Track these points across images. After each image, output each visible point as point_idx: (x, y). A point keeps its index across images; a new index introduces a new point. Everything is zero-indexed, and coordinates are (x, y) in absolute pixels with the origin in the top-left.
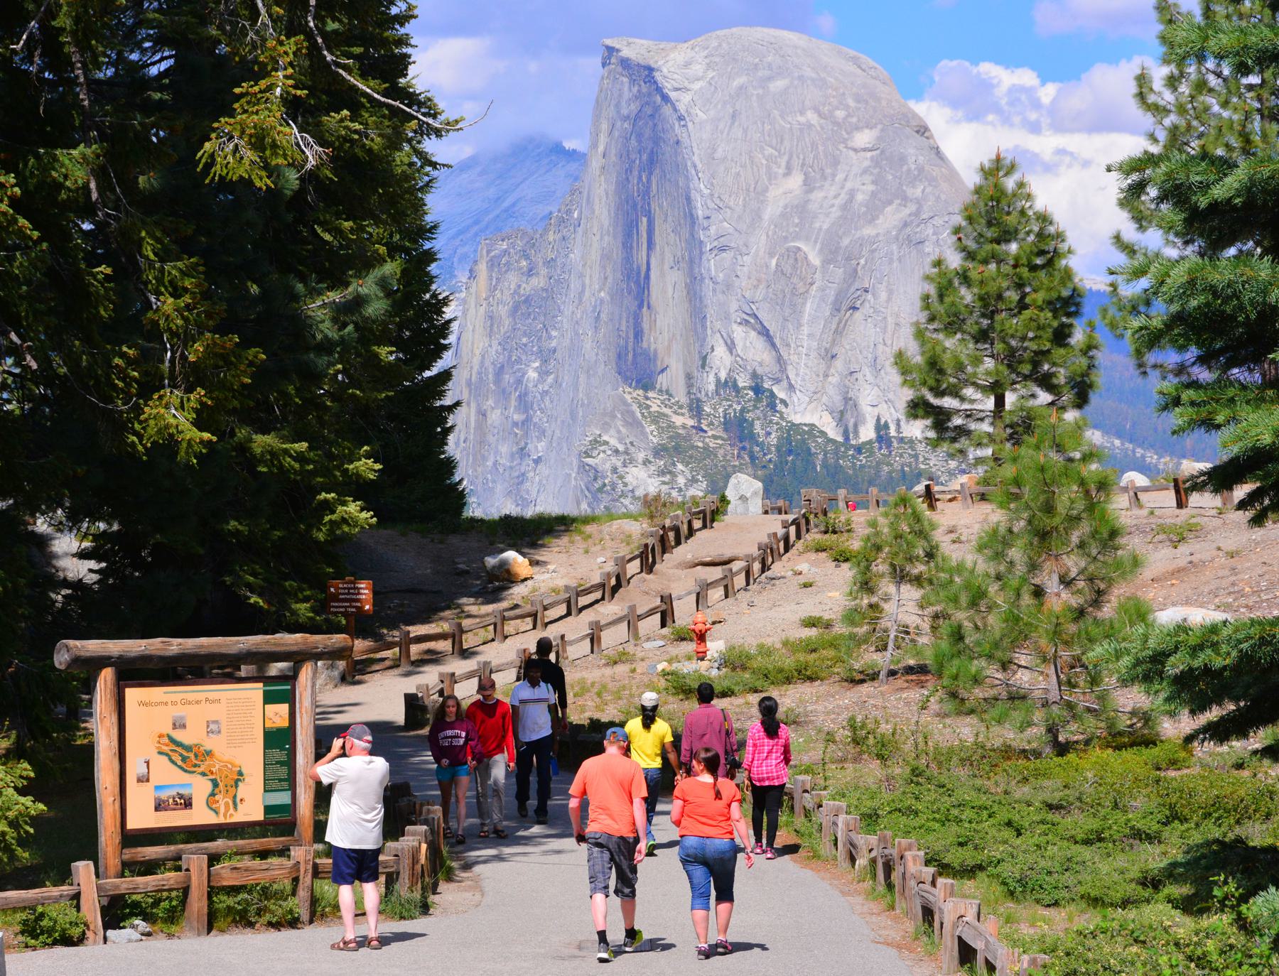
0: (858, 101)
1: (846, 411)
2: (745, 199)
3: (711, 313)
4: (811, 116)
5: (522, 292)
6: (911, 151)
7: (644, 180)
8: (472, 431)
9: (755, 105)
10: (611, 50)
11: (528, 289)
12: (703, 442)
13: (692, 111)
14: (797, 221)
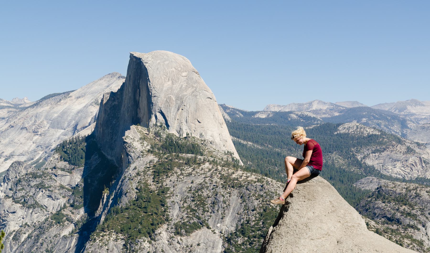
0: (184, 66)
1: (180, 131)
4: (174, 69)
7: (138, 81)
11: (113, 104)
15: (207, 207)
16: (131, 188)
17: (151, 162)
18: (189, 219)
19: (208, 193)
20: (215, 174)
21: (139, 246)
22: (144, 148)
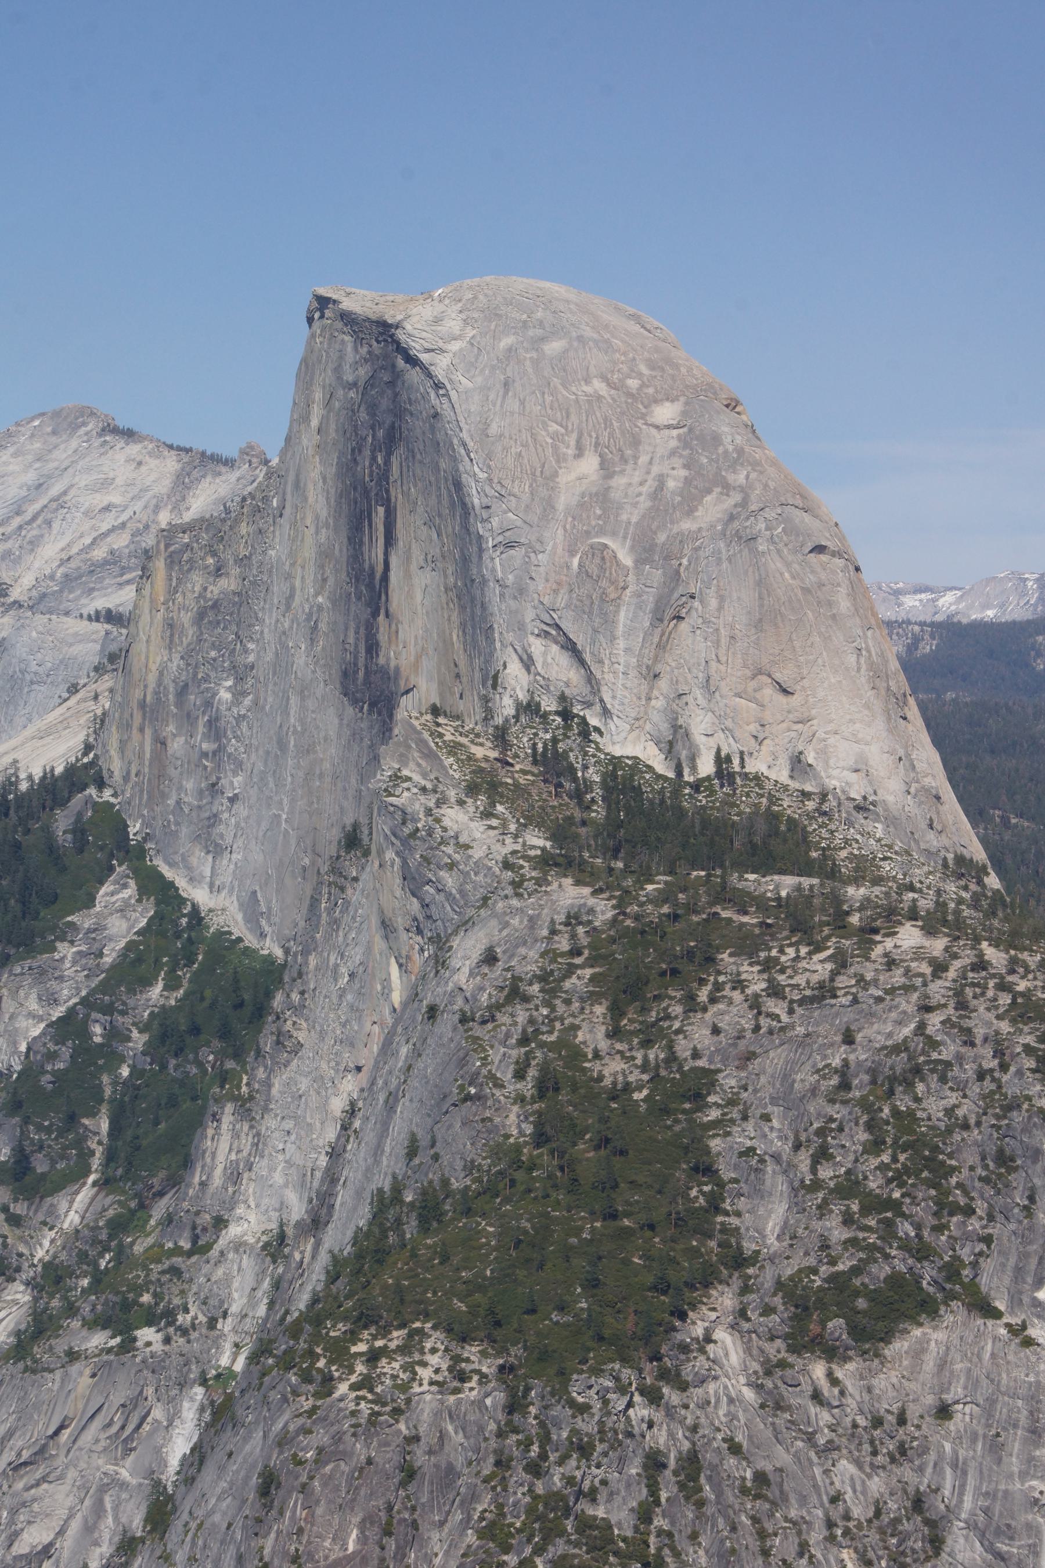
0: (653, 369)
2: (531, 486)
3: (499, 622)
4: (599, 386)
5: (209, 595)
6: (726, 429)
7: (380, 460)
8: (147, 763)
9: (530, 370)
10: (323, 302)
11: (216, 592)
12: (513, 778)
13: (453, 377)
14: (598, 512)
15: (960, 1185)
16: (484, 1072)
17: (573, 919)
18: (862, 1255)
19: (953, 1101)
20: (978, 990)
21: (596, 1418)
22: (510, 845)
